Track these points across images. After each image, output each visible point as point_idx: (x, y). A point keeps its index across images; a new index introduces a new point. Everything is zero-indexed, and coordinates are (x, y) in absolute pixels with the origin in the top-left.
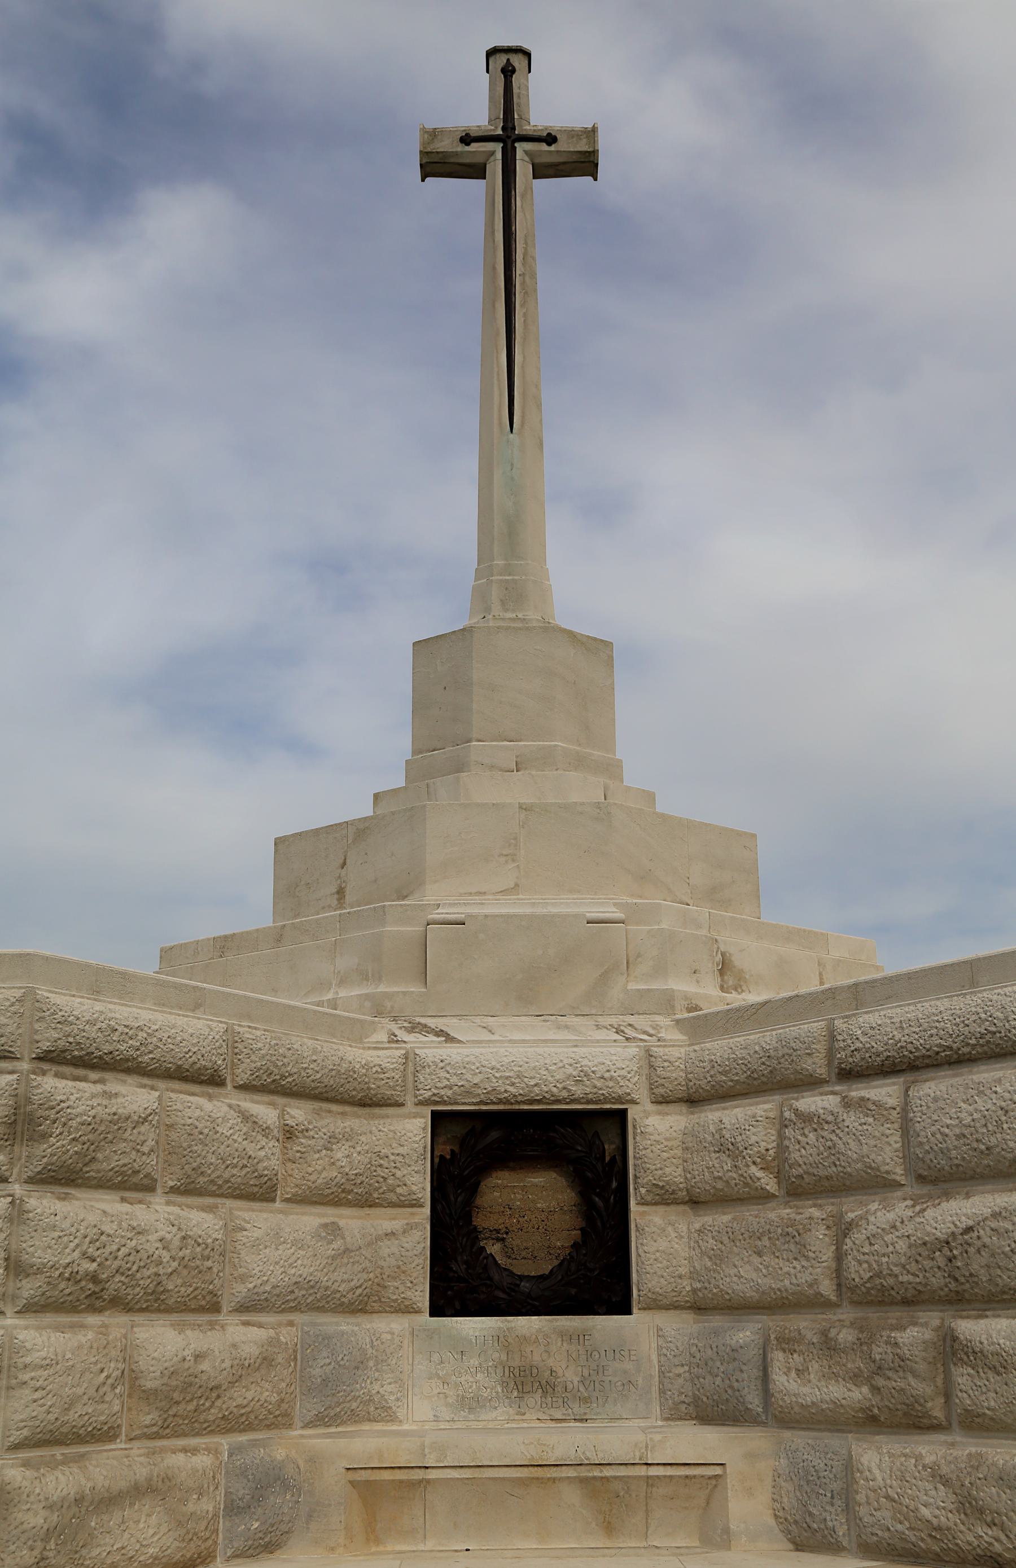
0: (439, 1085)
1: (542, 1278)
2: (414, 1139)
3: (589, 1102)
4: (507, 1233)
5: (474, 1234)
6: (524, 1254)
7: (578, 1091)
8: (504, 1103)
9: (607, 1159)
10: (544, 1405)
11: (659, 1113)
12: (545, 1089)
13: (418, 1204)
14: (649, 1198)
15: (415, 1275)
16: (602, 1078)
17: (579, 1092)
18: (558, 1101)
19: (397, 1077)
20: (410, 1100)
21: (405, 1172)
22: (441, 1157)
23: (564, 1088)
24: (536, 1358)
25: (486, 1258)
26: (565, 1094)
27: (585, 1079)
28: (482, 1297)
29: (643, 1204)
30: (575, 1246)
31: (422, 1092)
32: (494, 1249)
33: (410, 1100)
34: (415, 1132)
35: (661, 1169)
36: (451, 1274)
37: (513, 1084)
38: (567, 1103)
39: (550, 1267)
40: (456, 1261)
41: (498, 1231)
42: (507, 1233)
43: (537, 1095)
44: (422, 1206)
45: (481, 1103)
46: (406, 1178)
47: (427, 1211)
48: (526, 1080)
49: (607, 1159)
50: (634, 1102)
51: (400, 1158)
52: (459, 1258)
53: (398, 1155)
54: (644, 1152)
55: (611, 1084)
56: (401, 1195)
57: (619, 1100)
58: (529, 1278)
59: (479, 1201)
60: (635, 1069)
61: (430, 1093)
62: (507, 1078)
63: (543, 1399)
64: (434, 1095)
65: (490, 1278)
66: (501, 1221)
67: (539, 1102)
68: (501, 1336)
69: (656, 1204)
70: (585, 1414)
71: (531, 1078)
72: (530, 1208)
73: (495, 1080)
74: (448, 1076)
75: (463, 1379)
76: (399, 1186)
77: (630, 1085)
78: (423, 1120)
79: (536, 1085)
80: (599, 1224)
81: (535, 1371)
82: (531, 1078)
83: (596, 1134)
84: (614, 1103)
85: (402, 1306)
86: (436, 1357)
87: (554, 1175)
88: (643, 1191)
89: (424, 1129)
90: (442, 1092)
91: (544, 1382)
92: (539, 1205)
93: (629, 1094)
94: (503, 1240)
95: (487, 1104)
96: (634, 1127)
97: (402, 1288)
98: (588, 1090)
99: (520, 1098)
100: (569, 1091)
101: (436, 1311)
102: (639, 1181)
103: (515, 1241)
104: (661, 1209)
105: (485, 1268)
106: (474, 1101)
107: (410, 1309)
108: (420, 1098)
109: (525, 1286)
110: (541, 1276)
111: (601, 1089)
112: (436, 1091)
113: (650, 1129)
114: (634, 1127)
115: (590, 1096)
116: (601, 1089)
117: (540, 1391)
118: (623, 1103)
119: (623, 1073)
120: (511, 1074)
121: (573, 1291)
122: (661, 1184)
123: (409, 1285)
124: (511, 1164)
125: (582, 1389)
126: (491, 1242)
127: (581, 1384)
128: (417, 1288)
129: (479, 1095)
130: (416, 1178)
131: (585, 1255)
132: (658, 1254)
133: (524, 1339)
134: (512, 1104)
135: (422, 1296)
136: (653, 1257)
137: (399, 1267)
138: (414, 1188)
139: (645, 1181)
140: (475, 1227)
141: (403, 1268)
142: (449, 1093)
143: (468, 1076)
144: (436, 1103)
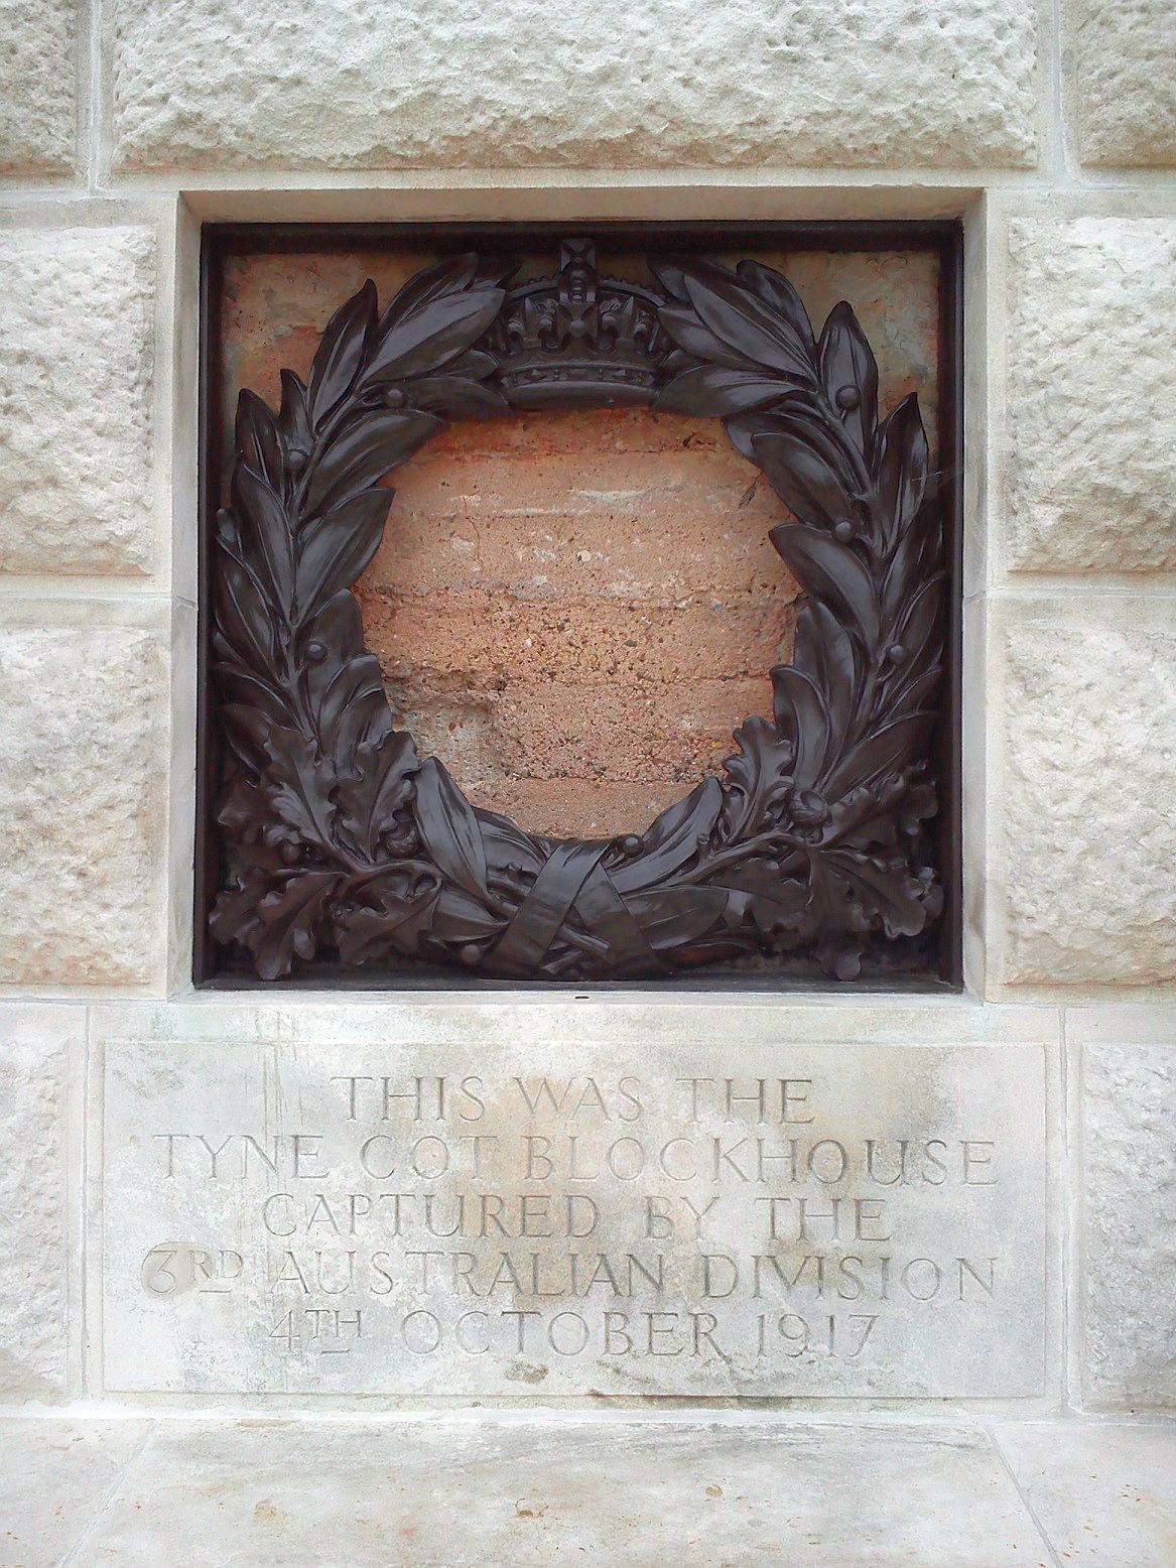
0: (199, 78)
1: (619, 851)
2: (95, 297)
3: (828, 158)
4: (500, 687)
5: (372, 690)
6: (560, 758)
7: (788, 104)
8: (478, 163)
9: (883, 414)
10: (620, 1345)
11: (1118, 209)
12: (647, 93)
13: (115, 564)
14: (1069, 548)
15: (95, 843)
16: (887, 45)
17: (787, 110)
18: (695, 153)
19: (32, 47)
20: (98, 154)
21: (54, 428)
22: (244, 395)
23: (726, 92)
24: (592, 1169)
25: (411, 776)
26: (727, 119)
27: (815, 52)
28: (391, 916)
29: (1042, 572)
30: (746, 734)
31: (134, 111)
32: (451, 744)
33: (98, 154)
34: (100, 270)
35: (1128, 424)
36: (276, 833)
37: (507, 73)
38: (738, 165)
39: (656, 808)
40: (297, 786)
41: (468, 680)
42: (500, 687)
43: (611, 121)
44: (134, 572)
45: (379, 158)
46: (52, 456)
47: (162, 590)
48: (564, 53)
49: (883, 414)
50: (1013, 162)
51: (30, 374)
52: (306, 775)
53: (22, 358)
54: (1058, 356)
55: (927, 74)
56: (39, 523)
57: (955, 147)
58: (574, 846)
59: (391, 567)
60: (1023, 20)
61: (165, 115)
62: (487, 44)
63: (617, 1322)
64: (182, 122)
65: (420, 850)
66: (477, 642)
67: (619, 154)
68: (454, 1080)
69: (1091, 571)
70: (782, 1377)
71: (587, 46)
72: (585, 601)
73: (429, 56)
74: (238, 41)
75: (297, 1242)
76: (27, 486)
77: (1007, 86)
78: (143, 232)
79: (605, 76)
80: (843, 651)
81: (583, 1213)
82: (587, 46)
83: (844, 315)
84: (931, 165)
85: (53, 965)
86: (192, 1157)
87: (677, 478)
88: (1046, 516)
89: (145, 263)
90: (216, 110)
91: (618, 1260)
92: (617, 588)
93: (996, 123)
94: (486, 708)
95: (404, 165)
96: (1013, 259)
97: (41, 898)
98: (826, 100)
99: (538, 139)
100: (748, 102)
101: (222, 960)
102: (1033, 476)
103: (522, 712)
104: (1113, 593)
105: (407, 812)
106: (352, 149)
107: (88, 975)
108: (130, 138)
109: (561, 873)
110: (617, 844)
111: (879, 96)
112: (189, 107)
113: (1087, 262)
114: (1013, 259)
115: (834, 130)
116: (879, 96)
117: (605, 1289)
118: (967, 165)
119: (979, 28)
120: (500, 29)
121: (738, 901)
122: (1127, 487)
123: (71, 882)
124: (517, 436)
125: (771, 1286)
126: (443, 718)
127: (766, 1268)
128: (107, 893)
129: (367, 121)
130: (104, 455)
131: (787, 770)
132: (1108, 775)
133: (538, 1091)
134: (509, 166)
135: (154, 913)
136: (1090, 785)
137: (24, 815)
138: (92, 496)
139: (1060, 474)
140: (374, 671)
141: (44, 817)
142: (244, 114)
143: (322, 40)
144: (199, 160)
